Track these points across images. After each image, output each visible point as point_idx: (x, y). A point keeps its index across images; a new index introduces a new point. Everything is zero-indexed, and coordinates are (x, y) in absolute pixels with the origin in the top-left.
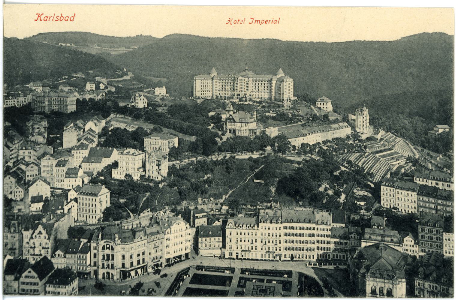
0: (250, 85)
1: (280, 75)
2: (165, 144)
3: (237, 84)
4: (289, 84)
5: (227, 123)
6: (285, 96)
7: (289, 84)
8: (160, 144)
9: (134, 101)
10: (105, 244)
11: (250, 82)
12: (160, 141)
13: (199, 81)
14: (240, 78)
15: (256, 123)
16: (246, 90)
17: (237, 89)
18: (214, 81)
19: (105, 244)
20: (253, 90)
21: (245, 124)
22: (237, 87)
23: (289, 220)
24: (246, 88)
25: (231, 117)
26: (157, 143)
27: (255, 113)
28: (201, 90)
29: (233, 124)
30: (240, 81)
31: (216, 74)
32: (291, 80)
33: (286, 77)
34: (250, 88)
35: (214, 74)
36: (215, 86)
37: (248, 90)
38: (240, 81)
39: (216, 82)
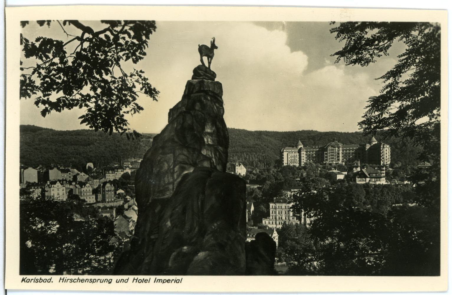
0: (341, 155)
1: (374, 143)
3: (326, 154)
4: (386, 150)
5: (357, 178)
6: (382, 163)
7: (386, 150)
11: (341, 152)
13: (287, 153)
14: (330, 148)
16: (336, 160)
18: (302, 153)
20: (343, 159)
21: (378, 179)
22: (326, 157)
24: (336, 159)
28: (289, 162)
29: (364, 179)
31: (302, 146)
32: (388, 146)
33: (383, 143)
34: (341, 158)
36: (302, 158)
37: (339, 160)
39: (303, 154)
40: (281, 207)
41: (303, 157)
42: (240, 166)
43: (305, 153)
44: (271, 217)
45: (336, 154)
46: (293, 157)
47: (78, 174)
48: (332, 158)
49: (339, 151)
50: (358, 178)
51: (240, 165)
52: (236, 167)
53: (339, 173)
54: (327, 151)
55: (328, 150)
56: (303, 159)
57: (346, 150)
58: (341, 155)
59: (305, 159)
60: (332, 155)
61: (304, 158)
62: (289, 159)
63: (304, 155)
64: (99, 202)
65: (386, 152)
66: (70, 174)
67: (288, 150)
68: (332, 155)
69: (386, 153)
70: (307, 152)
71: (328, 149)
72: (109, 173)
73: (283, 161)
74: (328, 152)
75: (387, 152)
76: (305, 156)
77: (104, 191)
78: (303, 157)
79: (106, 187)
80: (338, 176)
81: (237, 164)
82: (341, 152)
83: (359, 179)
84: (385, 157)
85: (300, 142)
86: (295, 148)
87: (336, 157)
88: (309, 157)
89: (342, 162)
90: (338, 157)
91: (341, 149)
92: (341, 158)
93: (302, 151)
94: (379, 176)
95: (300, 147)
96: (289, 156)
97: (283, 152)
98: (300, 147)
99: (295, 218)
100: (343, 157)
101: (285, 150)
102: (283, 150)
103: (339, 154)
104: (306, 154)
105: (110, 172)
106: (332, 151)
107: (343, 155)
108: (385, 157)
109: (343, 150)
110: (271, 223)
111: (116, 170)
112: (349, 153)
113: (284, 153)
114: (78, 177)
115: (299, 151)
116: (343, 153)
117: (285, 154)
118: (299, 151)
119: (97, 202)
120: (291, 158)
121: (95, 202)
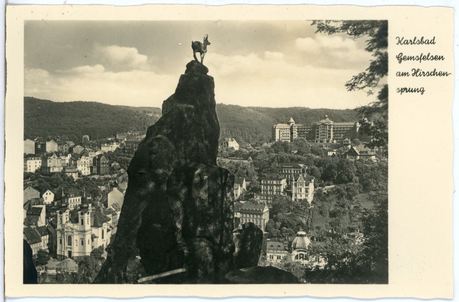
0: (332, 133)
2: (298, 172)
3: (318, 131)
5: (347, 156)
8: (293, 172)
9: (226, 145)
10: (299, 253)
11: (332, 129)
12: (293, 169)
13: (279, 129)
17: (318, 137)
18: (294, 129)
19: (299, 253)
20: (334, 137)
22: (318, 134)
24: (327, 136)
26: (289, 172)
31: (294, 123)
34: (332, 136)
35: (293, 123)
37: (330, 137)
39: (295, 131)
40: (273, 182)
41: (295, 133)
42: (233, 141)
43: (296, 130)
45: (327, 132)
46: (285, 134)
47: (74, 146)
48: (324, 135)
49: (330, 128)
50: (349, 155)
51: (232, 141)
53: (330, 150)
54: (318, 128)
55: (320, 127)
56: (295, 136)
57: (337, 128)
58: (332, 133)
59: (297, 136)
60: (323, 132)
61: (296, 135)
62: (281, 136)
63: (296, 132)
64: (95, 174)
66: (66, 146)
67: (280, 127)
68: (323, 132)
70: (298, 129)
71: (320, 126)
72: (105, 146)
73: (275, 137)
74: (320, 129)
76: (297, 133)
77: (99, 163)
78: (295, 133)
79: (101, 160)
80: (329, 153)
81: (230, 139)
82: (332, 129)
85: (292, 120)
86: (286, 125)
88: (300, 133)
89: (333, 139)
90: (330, 134)
91: (332, 126)
92: (332, 136)
93: (294, 127)
95: (291, 124)
96: (281, 133)
97: (275, 129)
98: (291, 124)
99: (286, 194)
100: (334, 134)
101: (277, 127)
102: (275, 127)
103: (330, 131)
104: (298, 131)
105: (106, 145)
107: (334, 133)
109: (334, 128)
110: (263, 198)
111: (112, 143)
112: (340, 131)
113: (276, 129)
114: (74, 149)
115: (291, 129)
116: (333, 131)
117: (277, 131)
118: (291, 129)
119: (92, 174)
121: (89, 173)
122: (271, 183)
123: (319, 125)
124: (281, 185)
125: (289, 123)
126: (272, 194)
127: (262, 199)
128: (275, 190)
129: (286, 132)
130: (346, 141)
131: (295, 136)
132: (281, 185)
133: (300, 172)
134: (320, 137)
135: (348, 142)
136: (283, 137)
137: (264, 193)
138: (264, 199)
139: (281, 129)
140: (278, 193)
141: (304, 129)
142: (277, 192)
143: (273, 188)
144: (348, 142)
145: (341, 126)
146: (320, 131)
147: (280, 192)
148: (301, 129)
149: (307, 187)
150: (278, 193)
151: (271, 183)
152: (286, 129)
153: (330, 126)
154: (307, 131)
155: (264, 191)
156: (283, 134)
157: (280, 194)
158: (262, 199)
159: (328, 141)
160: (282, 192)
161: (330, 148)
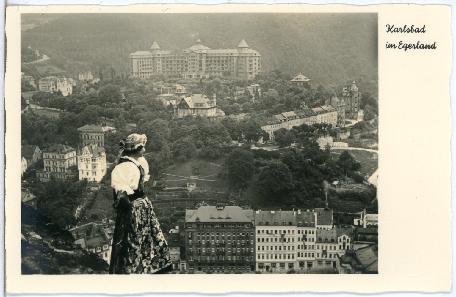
4: (255, 60)
7: (255, 60)
8: (94, 138)
15: (215, 109)
16: (198, 70)
17: (186, 69)
20: (207, 69)
22: (186, 66)
23: (264, 223)
24: (198, 68)
25: (183, 102)
27: (215, 96)
28: (140, 71)
30: (191, 58)
34: (204, 67)
37: (201, 69)
38: (191, 58)
40: (55, 156)
41: (159, 64)
42: (64, 82)
44: (45, 170)
49: (201, 58)
51: (62, 81)
52: (58, 84)
53: (171, 97)
58: (204, 63)
60: (194, 64)
62: (140, 68)
65: (255, 62)
69: (255, 64)
75: (257, 62)
78: (159, 64)
81: (58, 79)
82: (204, 59)
83: (182, 110)
84: (254, 68)
87: (198, 66)
89: (206, 72)
90: (201, 66)
91: (204, 55)
92: (204, 67)
94: (204, 107)
96: (140, 65)
103: (200, 61)
106: (194, 58)
108: (254, 68)
110: (46, 177)
120: (142, 66)
122: (54, 157)
123: (187, 54)
124: (66, 160)
125: (152, 51)
126: (55, 171)
127: (45, 178)
128: (58, 167)
129: (144, 63)
130: (179, 89)
131: (159, 68)
132: (66, 160)
133: (101, 137)
134: (189, 70)
135: (181, 92)
136: (143, 69)
137: (47, 169)
138: (47, 178)
139: (140, 59)
140: (63, 169)
141: (171, 58)
142: (61, 168)
143: (56, 164)
144: (181, 92)
145: (215, 54)
146: (189, 62)
147: (64, 168)
148: (168, 58)
149: (94, 163)
150: (63, 169)
151: (54, 157)
152: (148, 59)
153: (201, 54)
154: (175, 61)
155: (47, 167)
156: (143, 65)
157: (64, 170)
158: (45, 178)
159: (198, 76)
160: (67, 169)
161: (171, 95)
